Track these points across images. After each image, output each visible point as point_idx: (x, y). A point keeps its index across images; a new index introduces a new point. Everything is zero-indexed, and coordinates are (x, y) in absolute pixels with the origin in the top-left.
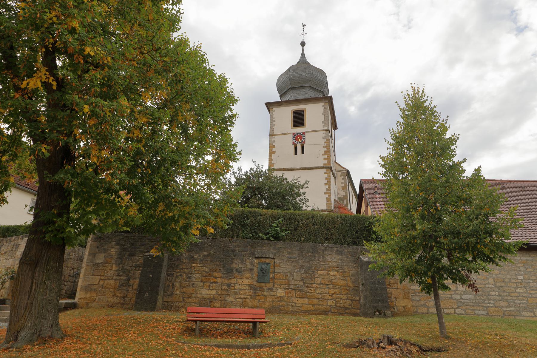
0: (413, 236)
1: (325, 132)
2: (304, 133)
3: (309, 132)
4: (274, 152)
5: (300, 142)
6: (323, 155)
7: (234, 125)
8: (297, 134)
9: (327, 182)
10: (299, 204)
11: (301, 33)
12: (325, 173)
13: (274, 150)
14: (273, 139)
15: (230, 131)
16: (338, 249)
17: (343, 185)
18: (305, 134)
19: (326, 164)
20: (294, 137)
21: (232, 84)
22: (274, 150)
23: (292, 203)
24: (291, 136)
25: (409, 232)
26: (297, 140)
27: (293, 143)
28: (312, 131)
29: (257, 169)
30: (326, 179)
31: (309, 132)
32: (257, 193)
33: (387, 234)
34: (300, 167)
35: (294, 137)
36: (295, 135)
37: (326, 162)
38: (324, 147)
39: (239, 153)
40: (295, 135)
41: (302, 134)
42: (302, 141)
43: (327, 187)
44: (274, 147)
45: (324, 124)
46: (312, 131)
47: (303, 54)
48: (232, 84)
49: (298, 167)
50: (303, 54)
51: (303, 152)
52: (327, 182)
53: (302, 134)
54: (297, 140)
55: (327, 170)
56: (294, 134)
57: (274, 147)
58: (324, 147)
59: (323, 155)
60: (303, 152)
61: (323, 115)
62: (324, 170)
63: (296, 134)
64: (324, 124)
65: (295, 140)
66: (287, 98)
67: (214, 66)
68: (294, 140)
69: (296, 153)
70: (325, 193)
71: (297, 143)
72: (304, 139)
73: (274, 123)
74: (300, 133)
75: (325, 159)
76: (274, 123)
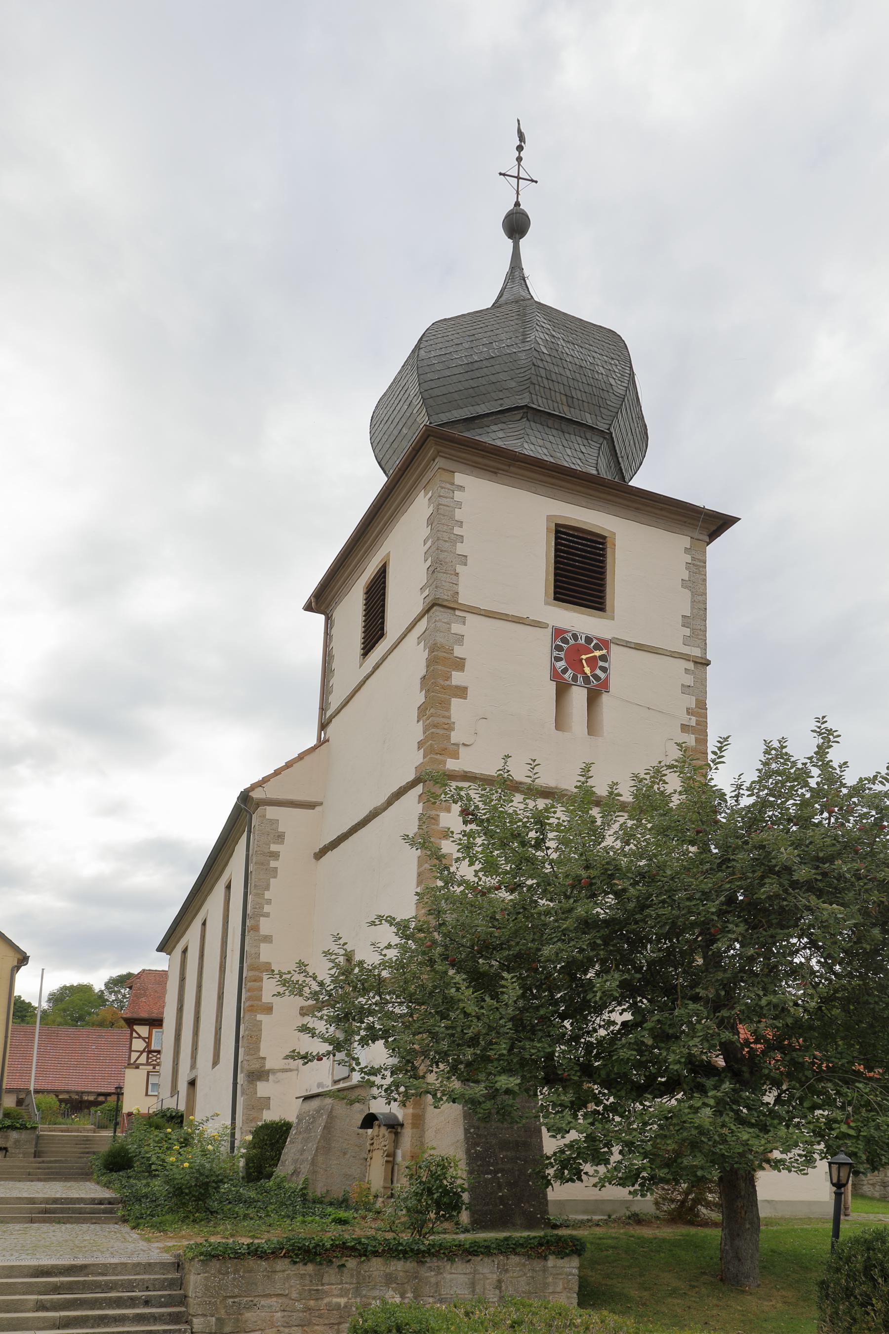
1: (691, 666)
2: (604, 644)
4: (462, 692)
8: (575, 637)
13: (457, 678)
14: (456, 628)
20: (559, 648)
22: (457, 678)
27: (555, 675)
28: (639, 647)
36: (565, 641)
40: (565, 641)
42: (597, 678)
45: (687, 632)
46: (639, 647)
54: (575, 664)
56: (558, 633)
57: (460, 664)
63: (568, 636)
65: (561, 665)
68: (558, 659)
71: (575, 679)
72: (604, 670)
73: (461, 549)
74: (589, 640)
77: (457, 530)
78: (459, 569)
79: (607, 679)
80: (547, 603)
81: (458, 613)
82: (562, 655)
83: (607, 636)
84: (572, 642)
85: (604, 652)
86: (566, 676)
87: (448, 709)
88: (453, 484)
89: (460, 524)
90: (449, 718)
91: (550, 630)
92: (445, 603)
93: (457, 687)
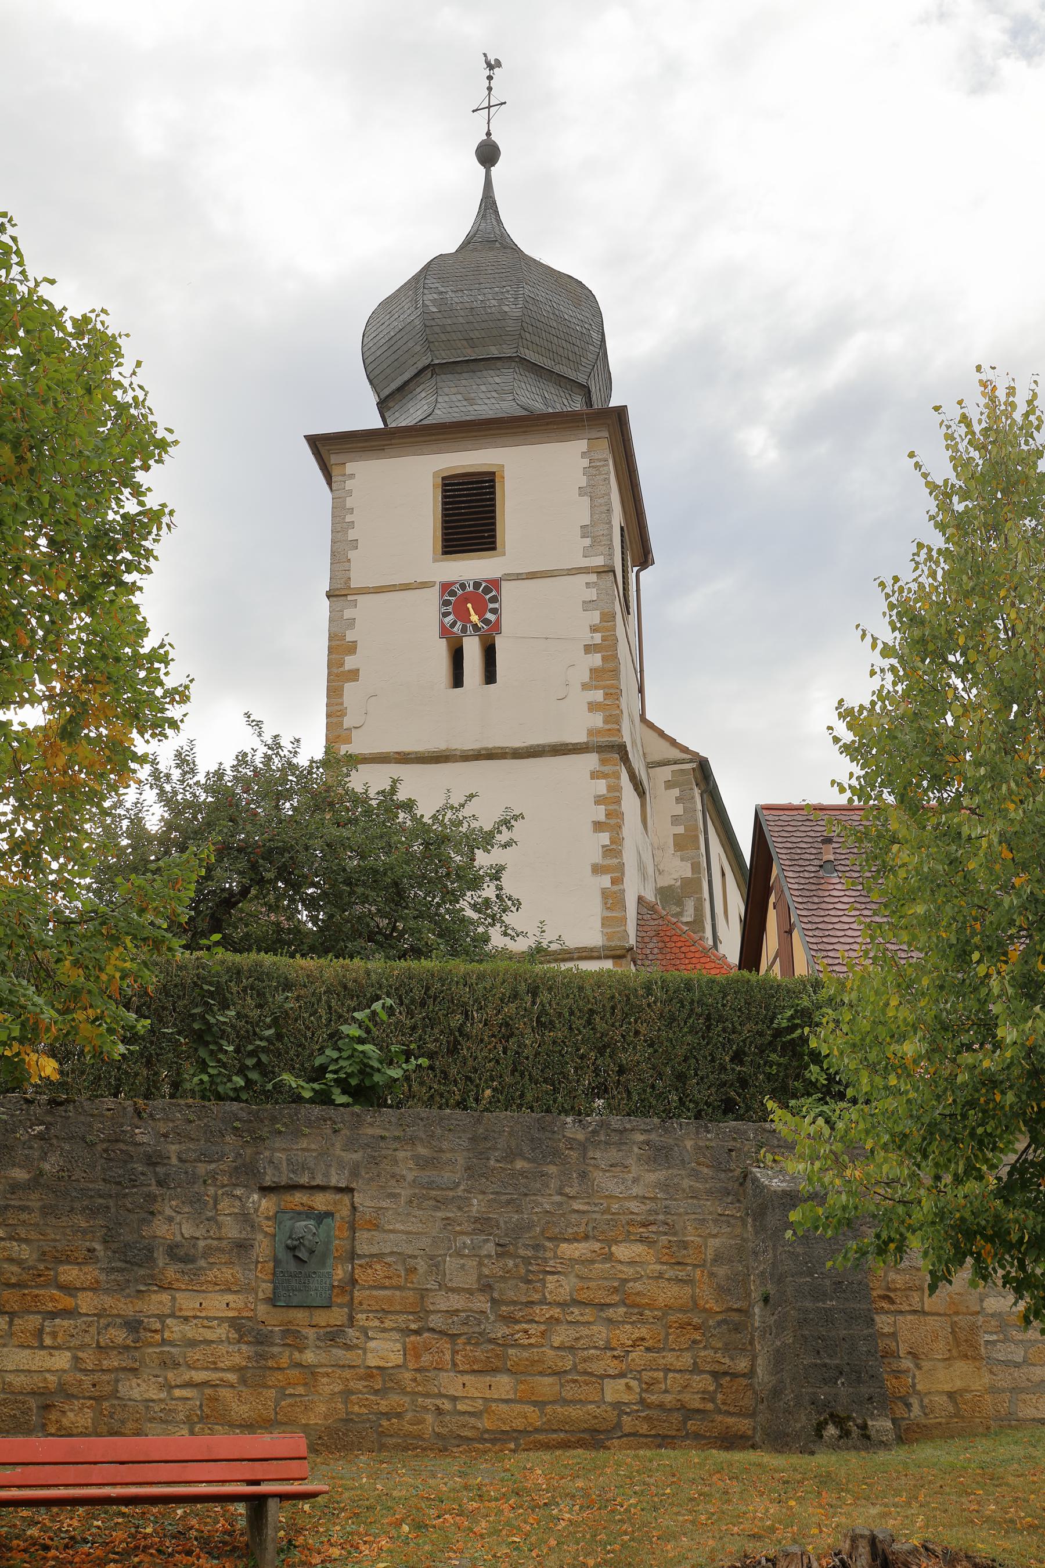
0: (982, 1073)
1: (593, 578)
2: (495, 584)
3: (518, 577)
4: (354, 675)
5: (475, 627)
6: (585, 687)
7: (152, 563)
8: (463, 586)
9: (602, 818)
10: (471, 922)
11: (479, 97)
12: (595, 775)
13: (350, 662)
14: (348, 614)
15: (133, 588)
16: (653, 1136)
17: (680, 830)
18: (498, 588)
19: (599, 732)
21: (139, 364)
22: (350, 662)
23: (435, 919)
24: (432, 598)
25: (967, 1058)
26: (464, 616)
28: (532, 576)
29: (268, 759)
30: (599, 800)
31: (518, 577)
32: (269, 875)
33: (873, 1068)
34: (476, 746)
35: (446, 603)
36: (453, 593)
37: (597, 720)
38: (588, 649)
39: (180, 695)
40: (453, 593)
41: (487, 590)
42: (487, 622)
43: (605, 838)
44: (352, 648)
45: (588, 542)
46: (532, 576)
47: (488, 204)
48: (139, 364)
49: (470, 744)
50: (488, 204)
51: (490, 676)
52: (602, 818)
53: (487, 590)
55: (603, 762)
56: (446, 588)
57: (352, 648)
58: (588, 649)
59: (585, 687)
60: (490, 676)
61: (586, 500)
62: (591, 760)
63: (456, 588)
64: (588, 542)
65: (451, 618)
66: (411, 414)
67: (52, 282)
68: (445, 615)
69: (457, 680)
70: (597, 870)
71: (464, 629)
72: (494, 611)
73: (352, 535)
74: (477, 585)
75: (593, 707)
76: (352, 535)
77: (349, 518)
78: (351, 554)
79: (498, 621)
80: (435, 560)
81: (349, 598)
82: (450, 609)
83: (497, 575)
84: (460, 592)
85: (494, 593)
86: (455, 629)
87: (341, 696)
88: (345, 475)
89: (351, 511)
90: (342, 704)
91: (437, 587)
92: (337, 593)
93: (349, 671)
